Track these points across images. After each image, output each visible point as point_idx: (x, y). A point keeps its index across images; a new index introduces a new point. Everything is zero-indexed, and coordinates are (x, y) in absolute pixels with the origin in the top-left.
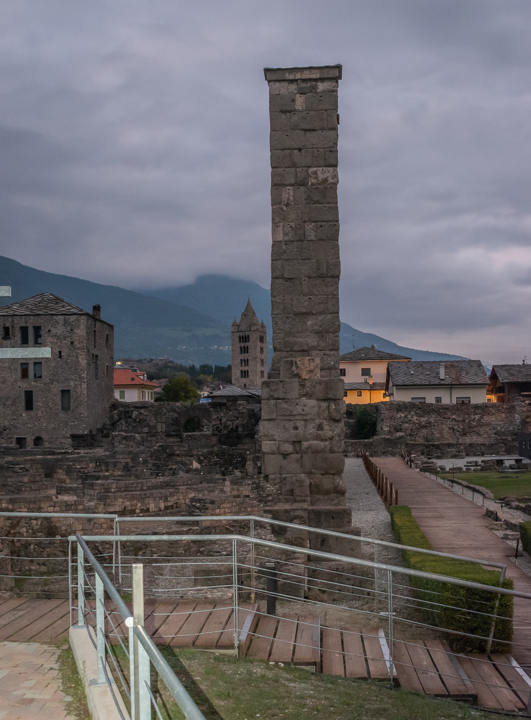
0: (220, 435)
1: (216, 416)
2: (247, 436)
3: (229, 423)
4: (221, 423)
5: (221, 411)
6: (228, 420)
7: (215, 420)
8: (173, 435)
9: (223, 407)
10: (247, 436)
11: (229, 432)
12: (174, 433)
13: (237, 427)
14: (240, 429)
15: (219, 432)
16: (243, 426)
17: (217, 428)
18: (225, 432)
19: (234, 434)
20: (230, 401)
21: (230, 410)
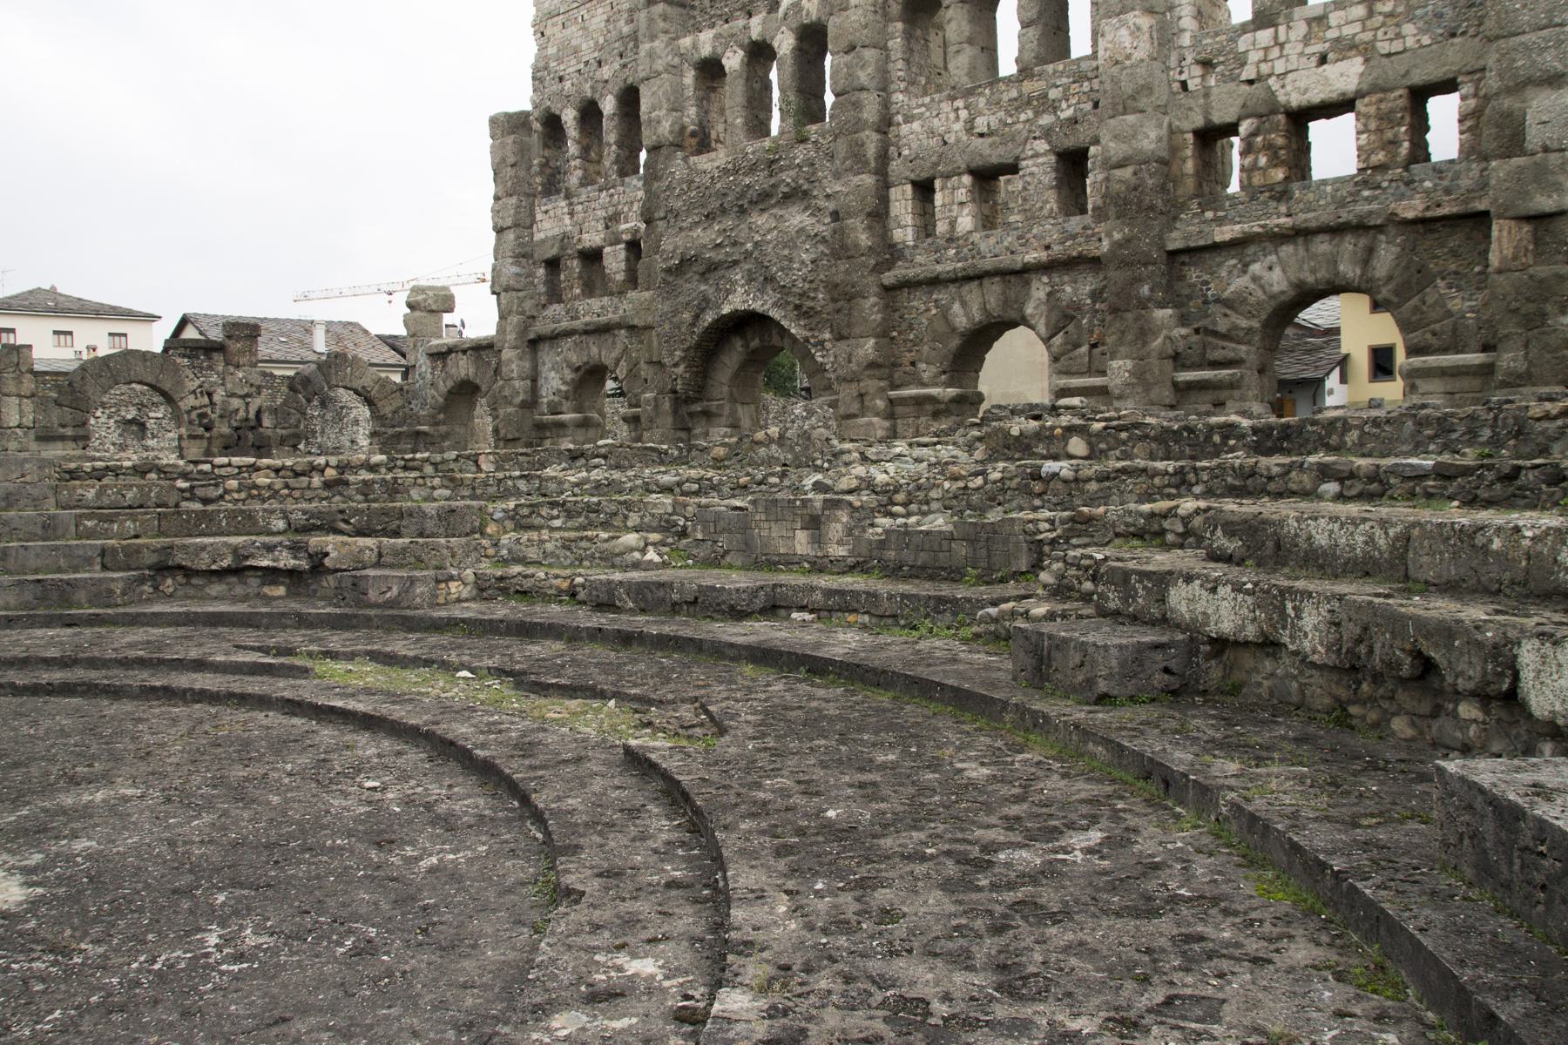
0: (210, 439)
1: (197, 383)
2: (283, 441)
3: (236, 403)
4: (212, 403)
5: (210, 368)
6: (233, 395)
7: (194, 392)
8: (63, 438)
9: (216, 356)
10: (283, 441)
11: (237, 429)
12: (69, 432)
13: (259, 413)
14: (267, 421)
15: (208, 429)
16: (274, 411)
17: (202, 416)
18: (225, 430)
19: (251, 436)
20: (238, 339)
21: (238, 366)
